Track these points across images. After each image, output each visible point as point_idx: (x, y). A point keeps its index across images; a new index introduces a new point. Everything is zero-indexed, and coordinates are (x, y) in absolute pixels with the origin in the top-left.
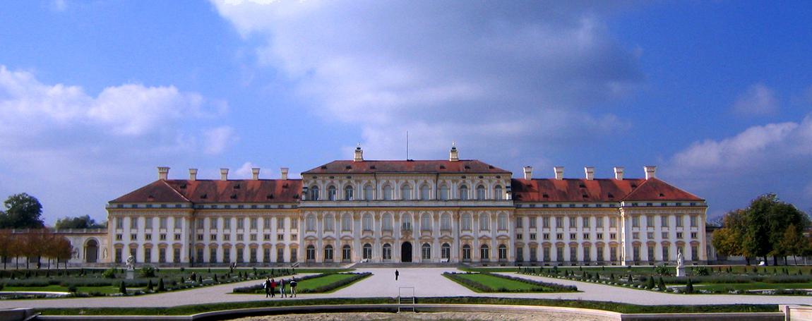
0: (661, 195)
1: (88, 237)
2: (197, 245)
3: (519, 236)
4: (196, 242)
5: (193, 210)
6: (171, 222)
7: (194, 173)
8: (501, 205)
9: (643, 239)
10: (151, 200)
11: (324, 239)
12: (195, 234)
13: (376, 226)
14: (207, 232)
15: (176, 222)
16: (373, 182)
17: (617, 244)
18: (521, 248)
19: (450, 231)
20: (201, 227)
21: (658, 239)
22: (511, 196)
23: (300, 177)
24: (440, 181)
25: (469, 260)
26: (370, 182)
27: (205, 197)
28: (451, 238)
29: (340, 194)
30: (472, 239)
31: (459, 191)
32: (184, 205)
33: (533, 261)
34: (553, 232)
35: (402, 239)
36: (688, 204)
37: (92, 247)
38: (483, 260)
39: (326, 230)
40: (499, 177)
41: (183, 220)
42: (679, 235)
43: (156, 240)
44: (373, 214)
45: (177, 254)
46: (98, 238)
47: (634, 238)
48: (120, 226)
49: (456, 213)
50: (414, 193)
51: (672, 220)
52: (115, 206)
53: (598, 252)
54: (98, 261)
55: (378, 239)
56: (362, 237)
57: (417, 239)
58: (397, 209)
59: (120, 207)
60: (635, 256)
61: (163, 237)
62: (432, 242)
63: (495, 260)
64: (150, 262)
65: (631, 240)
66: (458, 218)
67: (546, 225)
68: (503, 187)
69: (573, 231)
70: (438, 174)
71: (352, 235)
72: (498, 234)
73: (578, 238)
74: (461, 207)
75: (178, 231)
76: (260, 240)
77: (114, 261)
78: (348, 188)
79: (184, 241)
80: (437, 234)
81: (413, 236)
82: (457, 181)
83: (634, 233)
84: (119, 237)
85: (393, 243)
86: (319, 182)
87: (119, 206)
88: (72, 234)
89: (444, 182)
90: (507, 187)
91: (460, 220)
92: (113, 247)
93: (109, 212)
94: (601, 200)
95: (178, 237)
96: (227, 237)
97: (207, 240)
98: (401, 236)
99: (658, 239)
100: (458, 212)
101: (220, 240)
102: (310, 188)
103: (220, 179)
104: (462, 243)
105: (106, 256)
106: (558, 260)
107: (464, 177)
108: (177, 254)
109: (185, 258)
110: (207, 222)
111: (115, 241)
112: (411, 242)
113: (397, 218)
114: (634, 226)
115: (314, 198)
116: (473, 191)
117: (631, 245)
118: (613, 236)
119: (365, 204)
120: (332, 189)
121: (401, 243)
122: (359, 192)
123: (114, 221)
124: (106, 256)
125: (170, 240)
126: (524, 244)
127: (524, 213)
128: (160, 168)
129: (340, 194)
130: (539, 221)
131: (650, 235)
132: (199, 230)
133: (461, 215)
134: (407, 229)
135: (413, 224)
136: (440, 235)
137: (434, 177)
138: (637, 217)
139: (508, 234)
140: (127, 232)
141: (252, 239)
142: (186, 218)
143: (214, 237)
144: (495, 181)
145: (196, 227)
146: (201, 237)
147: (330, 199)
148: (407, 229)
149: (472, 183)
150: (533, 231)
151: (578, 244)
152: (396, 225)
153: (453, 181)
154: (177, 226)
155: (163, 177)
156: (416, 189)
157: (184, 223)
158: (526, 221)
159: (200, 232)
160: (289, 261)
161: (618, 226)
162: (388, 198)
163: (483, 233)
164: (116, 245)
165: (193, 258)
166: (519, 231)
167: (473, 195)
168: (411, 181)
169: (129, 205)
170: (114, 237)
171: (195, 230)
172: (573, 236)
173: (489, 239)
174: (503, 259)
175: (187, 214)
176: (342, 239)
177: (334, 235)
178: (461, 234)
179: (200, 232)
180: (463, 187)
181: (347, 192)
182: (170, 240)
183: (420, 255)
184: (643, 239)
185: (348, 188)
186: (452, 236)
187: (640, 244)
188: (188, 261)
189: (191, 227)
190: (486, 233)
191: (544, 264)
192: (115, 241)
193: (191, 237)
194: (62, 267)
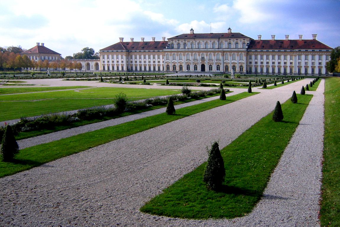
0: (313, 46)
1: (95, 62)
2: (130, 65)
3: (251, 63)
6: (120, 56)
7: (133, 39)
8: (210, 50)
9: (303, 64)
10: (113, 49)
11: (232, 63)
12: (130, 61)
14: (134, 60)
15: (112, 56)
16: (194, 41)
17: (293, 67)
18: (251, 67)
19: (220, 60)
20: (132, 58)
21: (310, 65)
22: (247, 47)
23: (167, 40)
24: (220, 41)
25: (228, 71)
26: (193, 42)
27: (133, 48)
28: (220, 63)
29: (182, 46)
30: (229, 63)
31: (228, 45)
33: (256, 72)
35: (201, 63)
36: (325, 50)
37: (97, 65)
38: (241, 71)
39: (173, 60)
40: (244, 39)
41: (124, 56)
42: (320, 63)
43: (115, 63)
44: (190, 54)
45: (122, 68)
46: (99, 62)
47: (299, 64)
48: (104, 58)
49: (222, 54)
50: (210, 46)
51: (317, 57)
52: (102, 51)
53: (284, 69)
55: (192, 63)
56: (186, 62)
57: (207, 63)
58: (199, 52)
59: (103, 52)
60: (298, 71)
62: (213, 64)
63: (238, 72)
64: (114, 70)
65: (297, 65)
66: (223, 55)
67: (262, 58)
68: (246, 43)
69: (154, 60)
70: (219, 38)
71: (183, 61)
72: (239, 62)
73: (281, 64)
74: (224, 51)
75: (122, 60)
76: (152, 63)
77: (102, 70)
78: (185, 44)
79: (125, 63)
81: (205, 62)
82: (227, 41)
83: (299, 62)
84: (104, 62)
85: (198, 64)
86: (174, 42)
87: (103, 51)
88: (90, 61)
89: (222, 41)
90: (247, 43)
94: (287, 48)
95: (122, 62)
96: (140, 62)
97: (134, 63)
98: (201, 62)
99: (310, 65)
100: (223, 53)
101: (138, 63)
102: (171, 44)
103: (141, 41)
104: (225, 65)
107: (230, 40)
108: (122, 68)
109: (125, 69)
110: (133, 57)
111: (102, 63)
112: (205, 64)
113: (199, 55)
114: (299, 59)
115: (172, 48)
116: (234, 45)
117: (297, 67)
118: (291, 63)
119: (198, 50)
120: (179, 44)
121: (201, 64)
122: (189, 46)
123: (102, 56)
124: (101, 68)
125: (120, 63)
126: (252, 66)
128: (120, 38)
129: (182, 46)
130: (259, 57)
131: (306, 63)
133: (224, 54)
134: (203, 59)
135: (205, 58)
136: (216, 62)
137: (217, 40)
138: (321, 56)
139: (244, 62)
141: (144, 63)
142: (125, 55)
143: (136, 62)
144: (243, 41)
145: (130, 58)
146: (132, 62)
147: (178, 48)
148: (203, 59)
149: (233, 42)
150: (256, 61)
151: (275, 66)
152: (199, 58)
153: (225, 41)
154: (122, 58)
156: (211, 44)
157: (124, 57)
158: (253, 57)
161: (294, 59)
162: (222, 48)
163: (233, 61)
165: (129, 69)
166: (250, 60)
167: (234, 46)
168: (209, 41)
169: (106, 51)
172: (268, 63)
173: (236, 63)
174: (168, 70)
176: (179, 63)
177: (176, 61)
178: (225, 62)
180: (230, 43)
181: (184, 46)
182: (120, 63)
184: (303, 64)
185: (185, 44)
186: (221, 62)
187: (301, 67)
189: (127, 58)
190: (235, 61)
192: (102, 63)
193: (127, 62)
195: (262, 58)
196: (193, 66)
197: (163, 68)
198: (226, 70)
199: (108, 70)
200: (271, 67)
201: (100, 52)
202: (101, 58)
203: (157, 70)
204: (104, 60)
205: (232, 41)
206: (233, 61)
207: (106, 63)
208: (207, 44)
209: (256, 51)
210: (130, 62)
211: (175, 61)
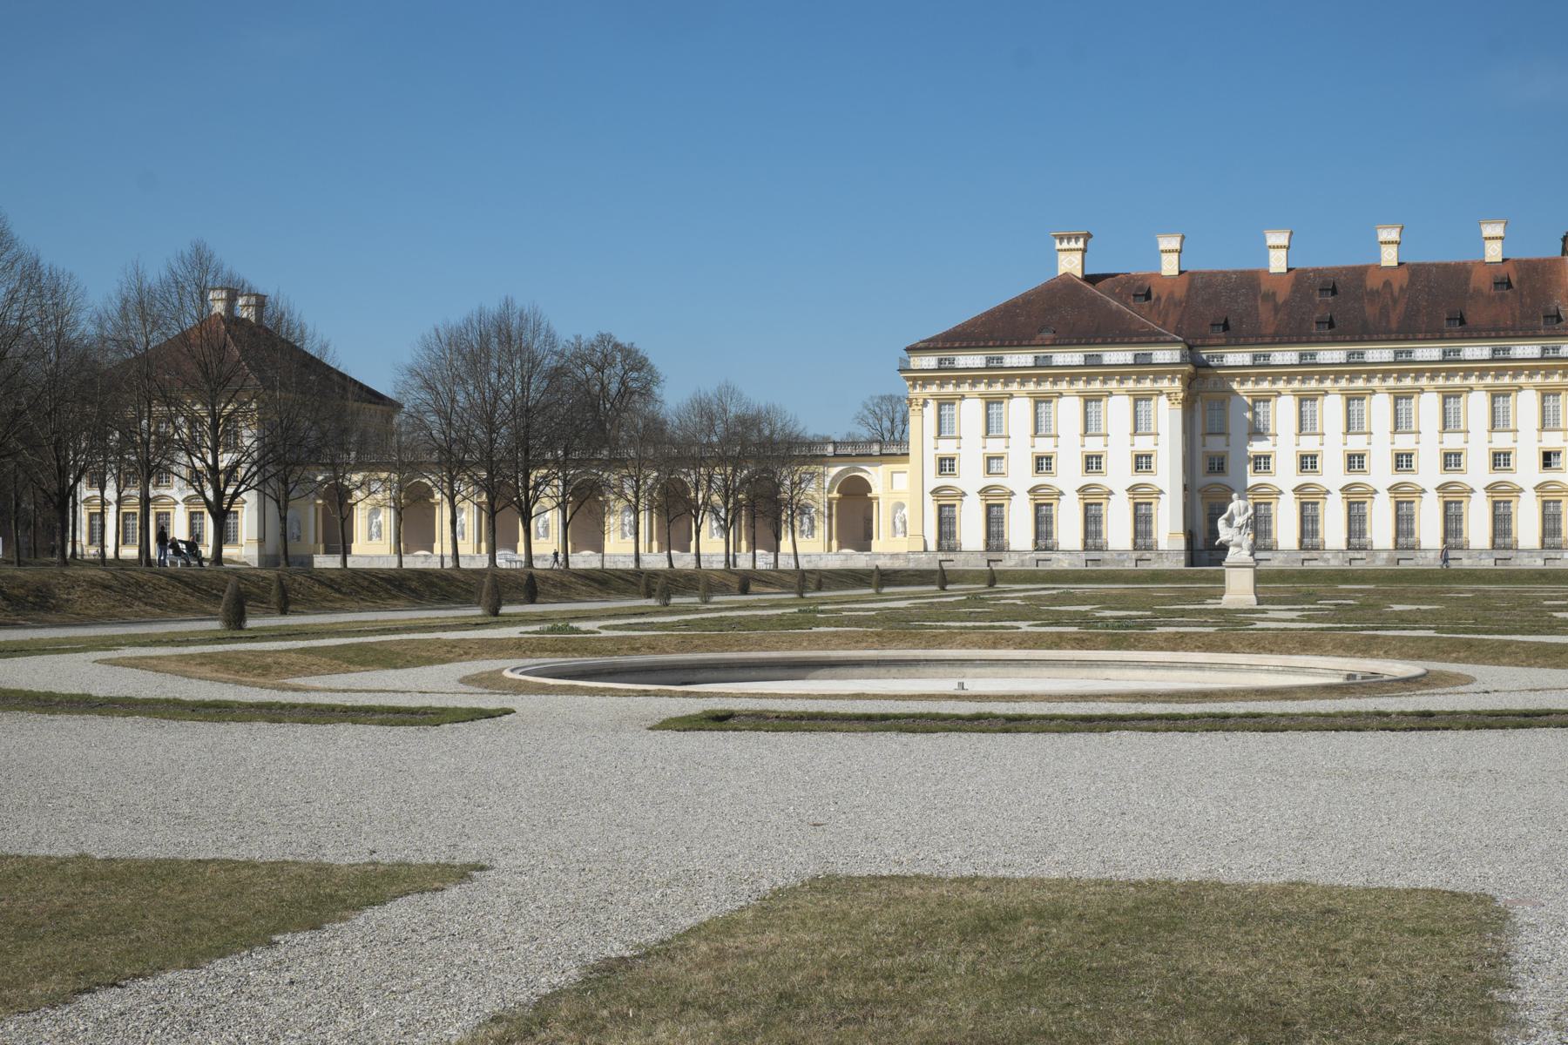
2: (1205, 491)
4: (1203, 479)
5: (1188, 368)
6: (1117, 409)
32: (1165, 355)
43: (1068, 476)
45: (1142, 521)
46: (877, 476)
52: (929, 361)
54: (877, 545)
61: (1092, 462)
75: (1144, 444)
77: (932, 546)
79: (1168, 476)
84: (946, 465)
92: (929, 498)
95: (1142, 462)
105: (901, 536)
108: (1142, 521)
123: (931, 410)
124: (901, 536)
125: (1118, 475)
132: (1210, 439)
140: (970, 450)
145: (1199, 429)
155: (1070, 264)
157: (1167, 416)
159: (1216, 445)
160: (1536, 544)
164: (935, 492)
169: (972, 360)
170: (931, 466)
171: (1198, 439)
175: (1177, 384)
179: (1216, 445)
182: (1118, 475)
188: (1180, 543)
194: (764, 560)
199: (988, 548)
202: (921, 425)
203: (1487, 544)
204: (947, 448)
207: (970, 477)
210: (1201, 465)
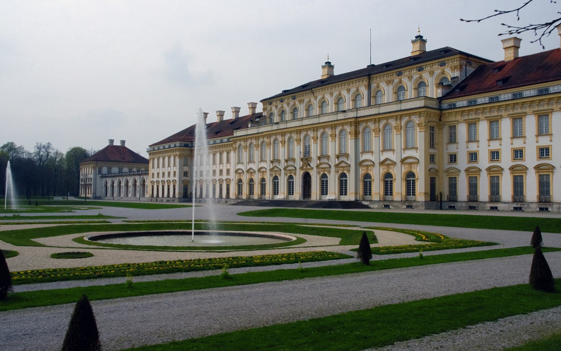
13: (282, 153)
19: (347, 156)
34: (506, 147)
35: (301, 168)
72: (404, 156)
80: (333, 161)
91: (360, 136)
93: (150, 155)
104: (362, 171)
106: (515, 201)
127: (459, 118)
133: (361, 130)
150: (473, 147)
183: (318, 192)
186: (349, 162)
191: (489, 205)
195: (493, 136)
196: (286, 178)
197: (228, 189)
198: (365, 193)
200: (534, 171)
201: (150, 153)
205: (405, 80)
206: (385, 153)
208: (358, 98)
209: (472, 103)
211: (251, 166)
